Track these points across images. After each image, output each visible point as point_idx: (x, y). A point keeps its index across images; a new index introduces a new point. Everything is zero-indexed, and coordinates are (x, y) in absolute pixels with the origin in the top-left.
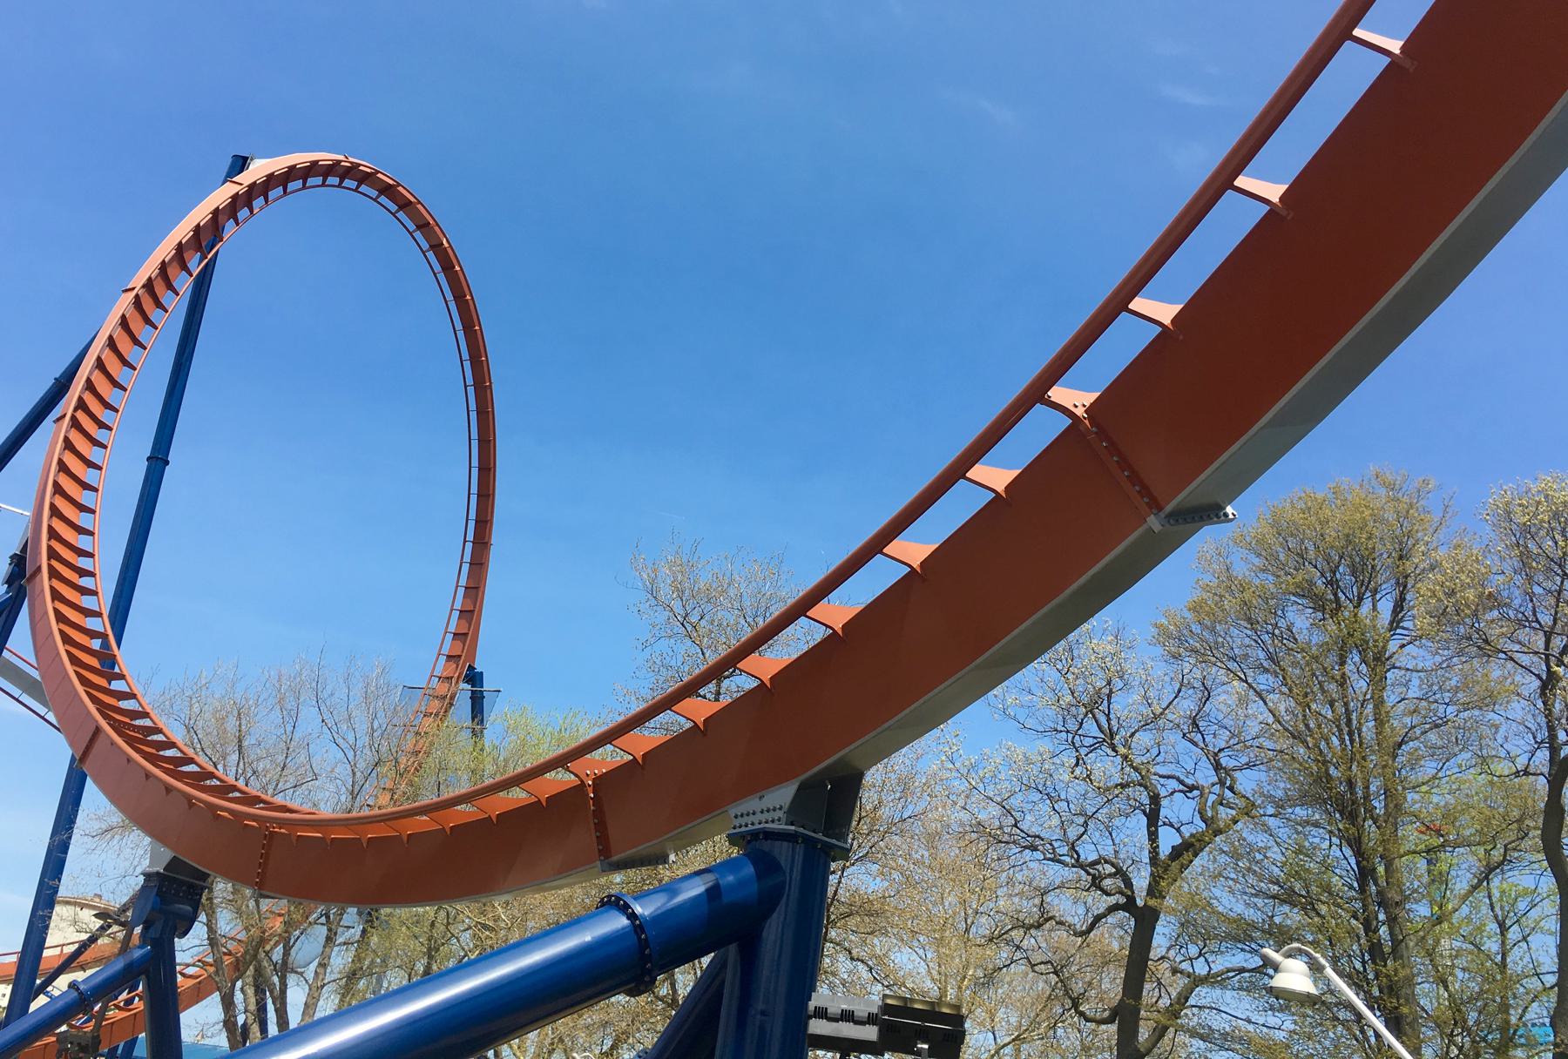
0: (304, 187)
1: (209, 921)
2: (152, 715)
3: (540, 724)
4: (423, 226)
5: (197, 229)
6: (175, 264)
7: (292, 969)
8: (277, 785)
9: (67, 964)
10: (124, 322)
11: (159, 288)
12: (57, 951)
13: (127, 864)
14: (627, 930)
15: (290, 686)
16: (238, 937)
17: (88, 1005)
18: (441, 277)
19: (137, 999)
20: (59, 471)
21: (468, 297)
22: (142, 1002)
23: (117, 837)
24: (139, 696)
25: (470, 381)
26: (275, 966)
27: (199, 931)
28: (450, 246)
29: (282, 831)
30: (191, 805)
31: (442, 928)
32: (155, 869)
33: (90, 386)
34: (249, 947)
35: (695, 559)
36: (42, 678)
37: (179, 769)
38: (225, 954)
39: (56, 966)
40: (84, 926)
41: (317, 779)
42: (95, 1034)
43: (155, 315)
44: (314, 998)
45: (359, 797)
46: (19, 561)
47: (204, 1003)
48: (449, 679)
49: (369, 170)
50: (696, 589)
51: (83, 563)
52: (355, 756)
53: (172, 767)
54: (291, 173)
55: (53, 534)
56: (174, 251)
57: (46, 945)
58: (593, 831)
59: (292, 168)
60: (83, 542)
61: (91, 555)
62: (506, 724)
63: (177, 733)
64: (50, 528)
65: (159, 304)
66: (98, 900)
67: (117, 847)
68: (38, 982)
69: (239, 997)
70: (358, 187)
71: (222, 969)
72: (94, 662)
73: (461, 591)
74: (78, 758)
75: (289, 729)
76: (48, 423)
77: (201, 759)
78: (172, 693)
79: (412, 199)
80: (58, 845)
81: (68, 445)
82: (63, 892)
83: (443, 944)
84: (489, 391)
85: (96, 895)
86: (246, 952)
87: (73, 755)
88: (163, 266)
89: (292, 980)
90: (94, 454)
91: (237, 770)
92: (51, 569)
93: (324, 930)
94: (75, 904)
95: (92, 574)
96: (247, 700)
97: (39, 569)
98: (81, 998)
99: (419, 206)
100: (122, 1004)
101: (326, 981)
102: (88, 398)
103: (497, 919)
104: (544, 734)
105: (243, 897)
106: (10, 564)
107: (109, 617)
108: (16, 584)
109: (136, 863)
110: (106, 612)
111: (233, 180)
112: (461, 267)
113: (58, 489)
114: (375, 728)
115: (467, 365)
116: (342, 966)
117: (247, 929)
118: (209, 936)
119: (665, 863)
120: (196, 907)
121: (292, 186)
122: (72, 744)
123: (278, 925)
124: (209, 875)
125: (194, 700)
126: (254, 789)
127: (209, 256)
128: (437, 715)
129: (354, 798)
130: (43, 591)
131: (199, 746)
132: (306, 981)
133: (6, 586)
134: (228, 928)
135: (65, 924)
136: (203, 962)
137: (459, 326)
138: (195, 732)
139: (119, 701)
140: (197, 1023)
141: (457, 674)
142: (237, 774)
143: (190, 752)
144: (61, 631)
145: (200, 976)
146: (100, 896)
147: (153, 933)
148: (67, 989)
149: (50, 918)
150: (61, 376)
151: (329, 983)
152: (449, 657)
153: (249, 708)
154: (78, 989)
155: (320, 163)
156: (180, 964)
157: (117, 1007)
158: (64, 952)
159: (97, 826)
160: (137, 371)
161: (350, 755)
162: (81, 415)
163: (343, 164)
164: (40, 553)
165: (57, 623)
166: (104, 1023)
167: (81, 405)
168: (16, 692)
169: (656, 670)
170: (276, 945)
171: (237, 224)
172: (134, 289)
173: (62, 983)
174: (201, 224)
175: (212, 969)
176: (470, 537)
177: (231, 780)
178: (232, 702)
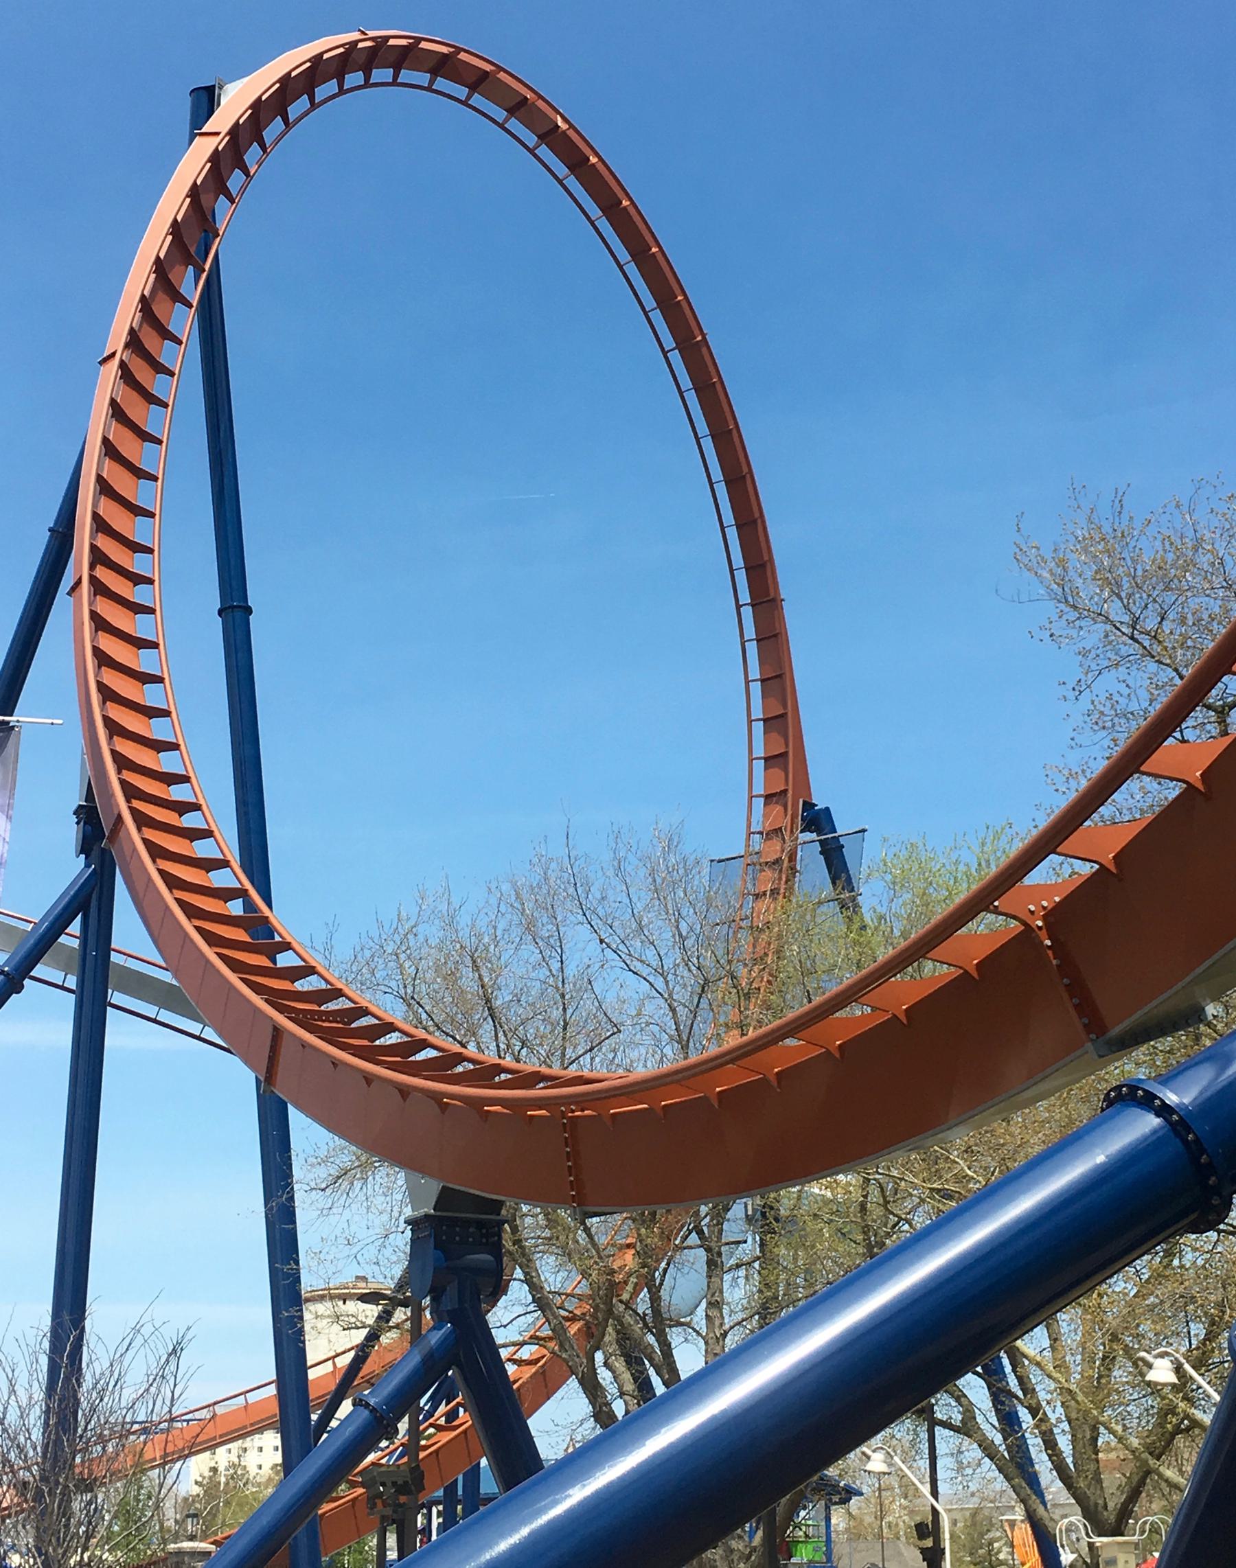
0: (314, 106)
1: (526, 1274)
2: (347, 991)
3: (944, 865)
4: (519, 107)
5: (176, 228)
6: (161, 295)
7: (671, 1320)
8: (563, 1054)
9: (347, 1382)
10: (117, 411)
11: (150, 340)
12: (328, 1367)
13: (385, 1217)
14: (1160, 1134)
15: (536, 900)
16: (577, 1291)
17: (388, 1425)
18: (573, 183)
19: (461, 1410)
20: (99, 667)
21: (625, 203)
22: (467, 1414)
23: (358, 1184)
24: (320, 969)
25: (669, 342)
26: (643, 1318)
27: (518, 1292)
28: (571, 126)
29: (587, 1112)
30: (444, 1107)
31: (879, 1211)
32: (423, 1211)
33: (100, 524)
34: (598, 1301)
35: (1125, 522)
36: (176, 976)
37: (412, 1058)
38: (567, 1319)
39: (333, 1388)
40: (353, 1320)
41: (619, 1031)
42: (413, 1465)
43: (159, 385)
44: (716, 1354)
45: (691, 1044)
46: (88, 815)
47: (558, 1395)
48: (778, 831)
49: (404, 42)
50: (1139, 573)
51: (178, 793)
52: (667, 983)
53: (399, 1059)
54: (287, 89)
55: (122, 763)
56: (153, 276)
57: (309, 1364)
58: (1066, 996)
59: (285, 80)
60: (168, 763)
61: (185, 779)
62: (888, 877)
63: (393, 1010)
64: (114, 753)
65: (159, 368)
66: (364, 1285)
67: (362, 1197)
68: (314, 1417)
69: (604, 1376)
70: (396, 76)
71: (568, 1339)
72: (240, 935)
73: (756, 688)
74: (262, 1079)
75: (555, 966)
76: (62, 605)
77: (438, 1039)
78: (368, 954)
79: (488, 68)
80: (279, 1210)
81: (100, 624)
82: (309, 1282)
83: (888, 1235)
84: (704, 350)
85: (357, 1277)
86: (596, 1308)
87: (256, 1077)
88: (145, 304)
89: (675, 1336)
90: (141, 626)
91: (498, 1046)
92: (136, 814)
93: (702, 1253)
94: (332, 1298)
95: (196, 807)
96: (479, 937)
97: (119, 818)
98: (376, 1417)
99: (502, 75)
100: (442, 1421)
101: (727, 1327)
102: (104, 543)
103: (962, 1178)
104: (955, 878)
105: (567, 1229)
106: (78, 823)
107: (242, 866)
108: (95, 853)
109: (396, 1214)
110: (234, 856)
111: (204, 130)
112: (597, 154)
113: (108, 694)
114: (684, 934)
115: (657, 317)
116: (745, 1302)
117: (585, 1274)
118: (533, 1296)
119: (1201, 1021)
120: (496, 1250)
121: (294, 110)
122: (247, 1062)
123: (629, 1260)
124: (501, 1203)
125: (403, 957)
126: (531, 1065)
127: (207, 267)
128: (774, 892)
129: (685, 1048)
130: (135, 850)
131: (431, 1023)
132: (698, 1333)
133: (83, 856)
134: (559, 1279)
135: (325, 1321)
136: (538, 1338)
137: (624, 255)
138: (418, 1003)
139: (293, 983)
140: (557, 1425)
141: (789, 817)
142: (499, 1051)
143: (421, 1034)
144: (179, 901)
145: (538, 1360)
146: (364, 1279)
147: (449, 1303)
148: (352, 1408)
149: (301, 1318)
150: (56, 523)
151: (732, 1328)
152: (768, 798)
153: (487, 949)
154: (367, 1405)
155: (325, 56)
156: (505, 1346)
157: (439, 1428)
158: (339, 1365)
159: (323, 1174)
160: (160, 481)
161: (659, 983)
162: (102, 573)
163: (360, 45)
164: (113, 795)
165: (171, 892)
166: (422, 1455)
167: (98, 557)
168: (150, 1010)
169: (1109, 724)
170: (636, 1293)
171: (232, 201)
172: (113, 354)
173: (346, 1408)
174: (179, 219)
175: (551, 1345)
176: (745, 597)
177: (490, 1057)
178: (458, 946)
